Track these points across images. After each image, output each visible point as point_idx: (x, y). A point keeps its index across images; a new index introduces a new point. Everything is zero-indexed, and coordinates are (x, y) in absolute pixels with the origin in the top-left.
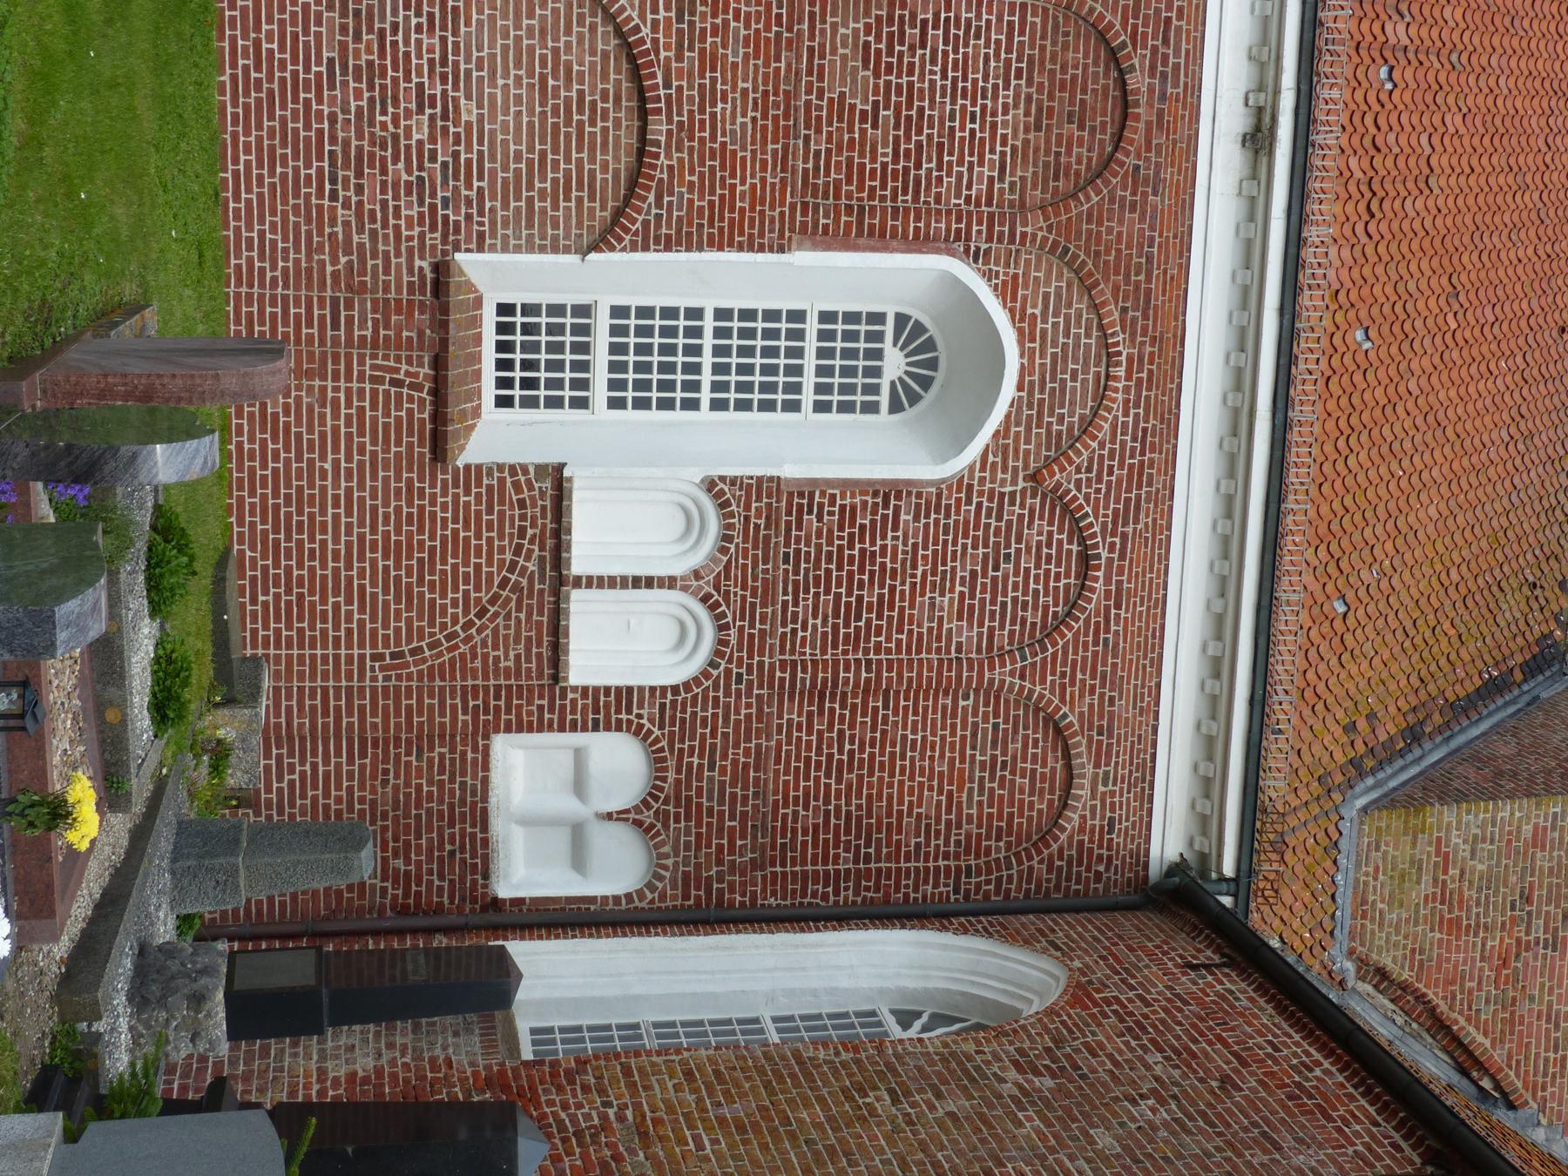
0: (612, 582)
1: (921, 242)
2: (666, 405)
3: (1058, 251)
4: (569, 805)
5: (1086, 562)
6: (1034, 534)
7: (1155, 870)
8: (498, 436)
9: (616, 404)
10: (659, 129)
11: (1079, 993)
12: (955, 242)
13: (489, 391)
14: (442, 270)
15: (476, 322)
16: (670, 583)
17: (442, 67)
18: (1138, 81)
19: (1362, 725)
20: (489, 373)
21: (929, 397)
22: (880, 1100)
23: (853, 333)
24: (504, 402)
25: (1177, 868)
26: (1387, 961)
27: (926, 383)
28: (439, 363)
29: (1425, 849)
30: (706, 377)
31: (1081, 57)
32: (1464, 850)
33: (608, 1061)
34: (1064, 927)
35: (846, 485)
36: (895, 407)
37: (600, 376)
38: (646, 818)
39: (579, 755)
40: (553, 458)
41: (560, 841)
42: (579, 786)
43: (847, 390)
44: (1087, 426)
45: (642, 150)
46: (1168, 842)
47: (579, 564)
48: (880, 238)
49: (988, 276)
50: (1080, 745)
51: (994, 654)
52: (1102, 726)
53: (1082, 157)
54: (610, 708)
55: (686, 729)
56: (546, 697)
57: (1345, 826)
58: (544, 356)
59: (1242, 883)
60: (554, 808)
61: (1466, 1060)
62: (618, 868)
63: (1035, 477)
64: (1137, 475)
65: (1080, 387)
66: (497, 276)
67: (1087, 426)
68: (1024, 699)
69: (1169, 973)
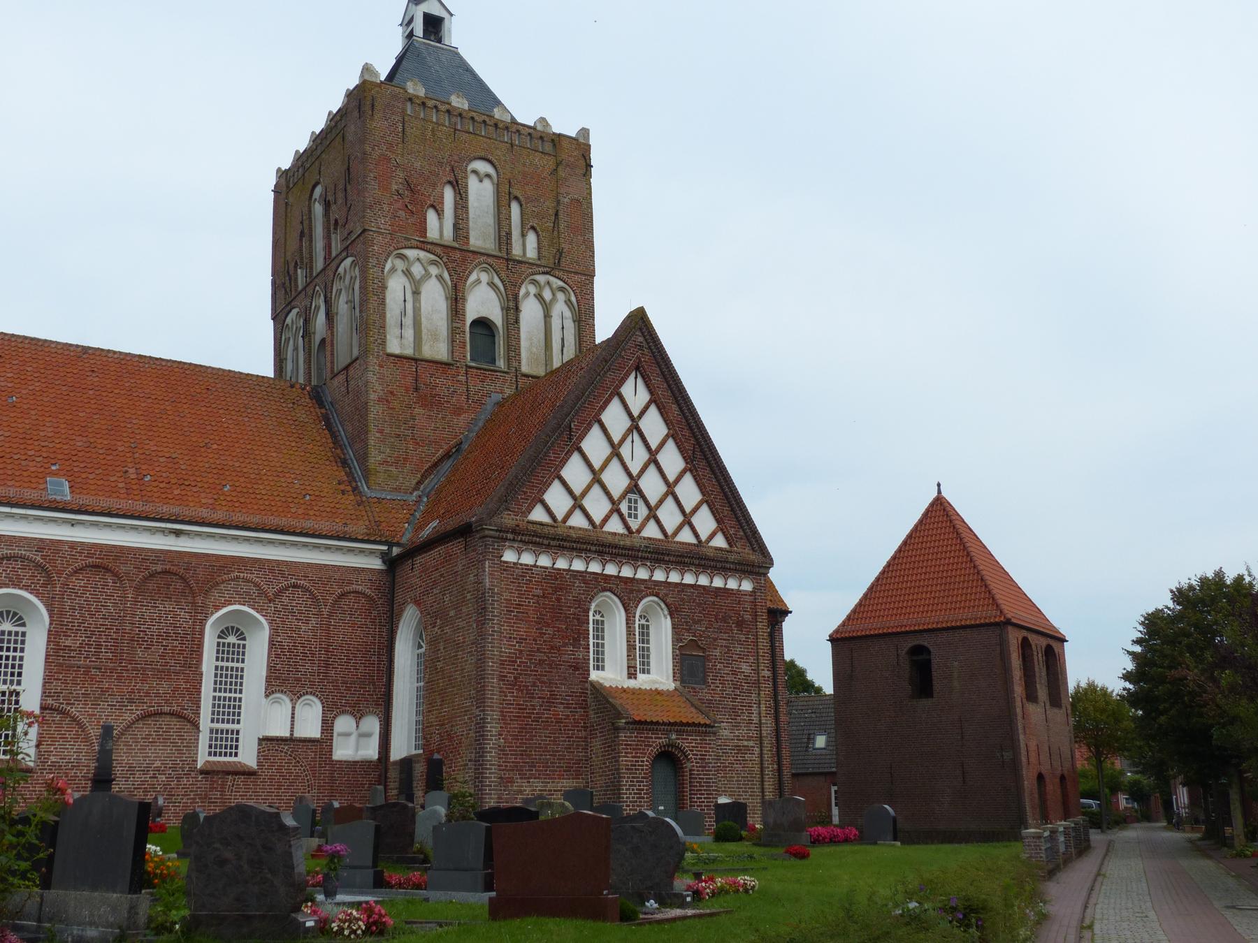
0: (292, 725)
1: (202, 633)
2: (240, 707)
3: (207, 593)
4: (353, 738)
5: (295, 586)
6: (286, 601)
7: (383, 567)
8: (248, 756)
9: (239, 722)
10: (166, 709)
11: (417, 603)
12: (202, 623)
13: (233, 759)
14: (202, 772)
15: (214, 762)
16: (293, 708)
17: (145, 772)
18: (159, 568)
19: (342, 487)
20: (228, 759)
21: (242, 629)
22: (440, 665)
23: (223, 651)
24: (236, 755)
25: (384, 562)
26: (414, 482)
27: (238, 630)
28: (228, 773)
29: (382, 468)
30: (233, 695)
31: (151, 585)
32: (383, 456)
33: (425, 731)
34: (399, 599)
35: (269, 657)
36: (244, 639)
37: (230, 726)
38: (359, 716)
39: (339, 735)
40: (256, 741)
41: (363, 740)
42: (348, 735)
43: (237, 653)
44: (256, 585)
45: (171, 714)
46: (376, 564)
47: (287, 734)
48: (200, 646)
49: (212, 614)
50: (347, 589)
51: (320, 614)
53: (180, 585)
54: (327, 726)
55: (335, 704)
56: (324, 744)
57: (373, 495)
58: (227, 741)
60: (354, 743)
61: (447, 456)
62: (372, 724)
63: (270, 601)
64: (272, 571)
65: (244, 587)
66: (203, 757)
67: (256, 585)
68: (333, 605)
69: (412, 576)
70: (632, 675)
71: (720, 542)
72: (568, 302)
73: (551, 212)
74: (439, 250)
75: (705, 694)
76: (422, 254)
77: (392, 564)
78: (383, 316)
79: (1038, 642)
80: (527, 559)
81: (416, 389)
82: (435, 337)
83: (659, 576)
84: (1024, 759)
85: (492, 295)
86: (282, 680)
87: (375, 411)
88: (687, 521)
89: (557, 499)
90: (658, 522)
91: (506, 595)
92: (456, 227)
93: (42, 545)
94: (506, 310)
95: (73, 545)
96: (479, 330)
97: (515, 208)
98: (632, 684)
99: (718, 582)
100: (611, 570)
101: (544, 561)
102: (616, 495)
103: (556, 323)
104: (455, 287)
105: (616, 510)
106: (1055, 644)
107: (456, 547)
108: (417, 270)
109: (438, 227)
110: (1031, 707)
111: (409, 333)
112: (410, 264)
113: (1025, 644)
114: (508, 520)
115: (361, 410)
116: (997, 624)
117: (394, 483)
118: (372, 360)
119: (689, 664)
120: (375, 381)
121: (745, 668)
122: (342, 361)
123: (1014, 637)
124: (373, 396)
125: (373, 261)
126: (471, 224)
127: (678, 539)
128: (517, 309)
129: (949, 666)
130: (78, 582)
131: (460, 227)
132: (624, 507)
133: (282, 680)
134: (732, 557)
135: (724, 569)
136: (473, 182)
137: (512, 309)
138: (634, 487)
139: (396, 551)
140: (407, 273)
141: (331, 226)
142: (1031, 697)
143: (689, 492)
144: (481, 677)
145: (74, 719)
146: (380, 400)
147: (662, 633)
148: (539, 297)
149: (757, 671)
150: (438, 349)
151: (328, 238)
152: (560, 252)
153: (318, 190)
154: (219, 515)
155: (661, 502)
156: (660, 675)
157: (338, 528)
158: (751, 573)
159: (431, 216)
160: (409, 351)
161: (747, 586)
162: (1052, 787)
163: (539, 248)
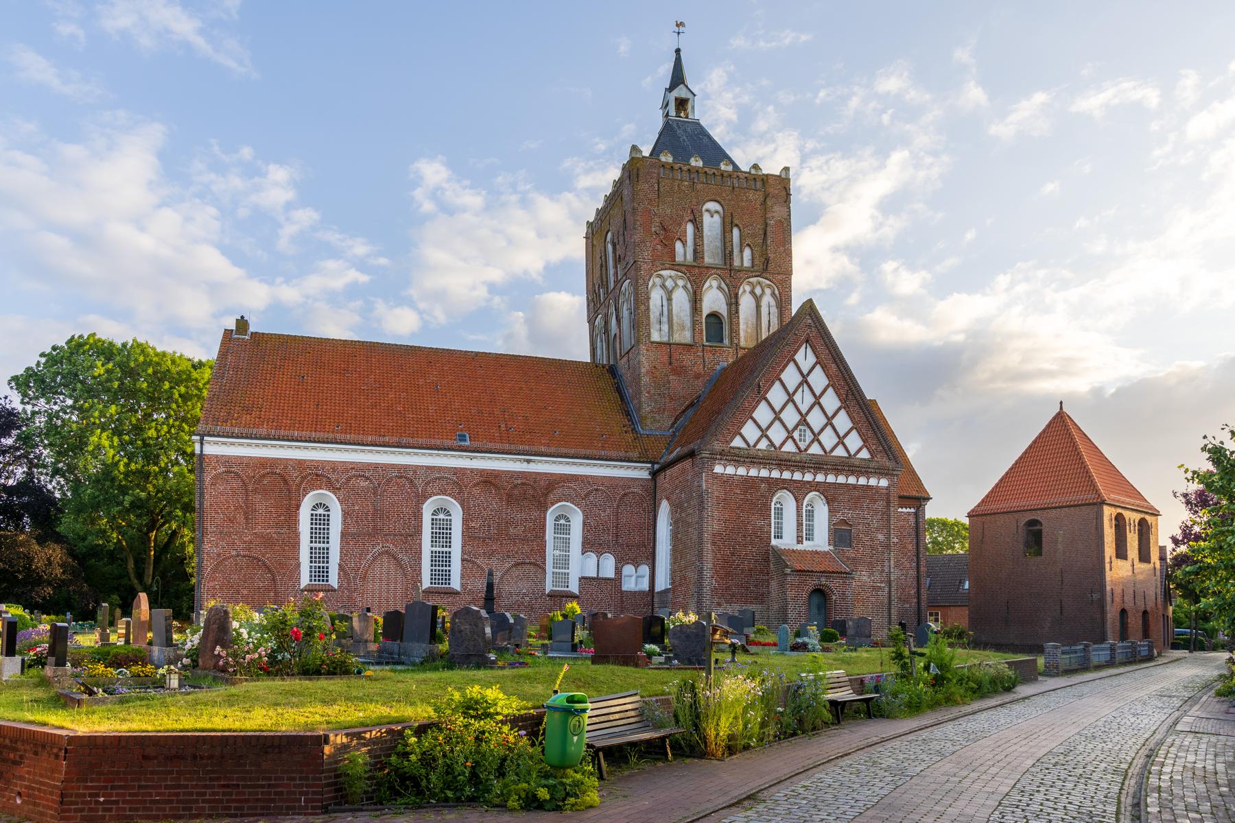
46: (645, 475)
48: (544, 526)
52: (624, 487)
59: (653, 463)
65: (567, 492)
70: (799, 541)
71: (864, 454)
72: (773, 294)
73: (761, 232)
74: (683, 269)
75: (851, 553)
76: (673, 273)
77: (654, 474)
78: (648, 317)
79: (1132, 517)
80: (730, 470)
81: (670, 364)
82: (683, 328)
83: (820, 478)
84: (1109, 599)
85: (721, 295)
86: (591, 544)
87: (645, 380)
88: (841, 441)
89: (750, 431)
90: (820, 443)
91: (716, 494)
92: (695, 251)
93: (456, 471)
94: (729, 305)
95: (472, 470)
96: (712, 320)
97: (736, 232)
98: (800, 547)
99: (862, 481)
100: (786, 475)
101: (742, 471)
102: (790, 427)
103: (764, 310)
104: (695, 292)
105: (790, 436)
106: (1148, 517)
107: (687, 464)
108: (669, 283)
109: (682, 252)
110: (1120, 562)
111: (665, 327)
112: (665, 280)
113: (1119, 519)
114: (717, 446)
115: (637, 379)
116: (1094, 504)
117: (656, 422)
118: (643, 347)
119: (840, 535)
120: (645, 360)
121: (881, 537)
122: (627, 346)
123: (1108, 512)
124: (643, 370)
125: (641, 281)
126: (705, 248)
127: (834, 454)
128: (737, 304)
129: (1057, 533)
130: (476, 491)
131: (698, 253)
132: (796, 435)
133: (591, 544)
134: (873, 465)
135: (867, 472)
136: (706, 218)
137: (733, 302)
138: (803, 421)
139: (656, 466)
140: (663, 286)
141: (618, 260)
142: (1121, 553)
143: (843, 422)
144: (701, 542)
145: (479, 566)
146: (647, 372)
147: (822, 513)
148: (752, 293)
149: (888, 539)
150: (685, 336)
151: (616, 267)
152: (767, 260)
153: (609, 235)
154: (552, 450)
155: (822, 430)
156: (820, 541)
157: (622, 454)
158: (887, 474)
159: (678, 245)
160: (665, 339)
161: (884, 483)
162: (1135, 622)
163: (753, 259)
